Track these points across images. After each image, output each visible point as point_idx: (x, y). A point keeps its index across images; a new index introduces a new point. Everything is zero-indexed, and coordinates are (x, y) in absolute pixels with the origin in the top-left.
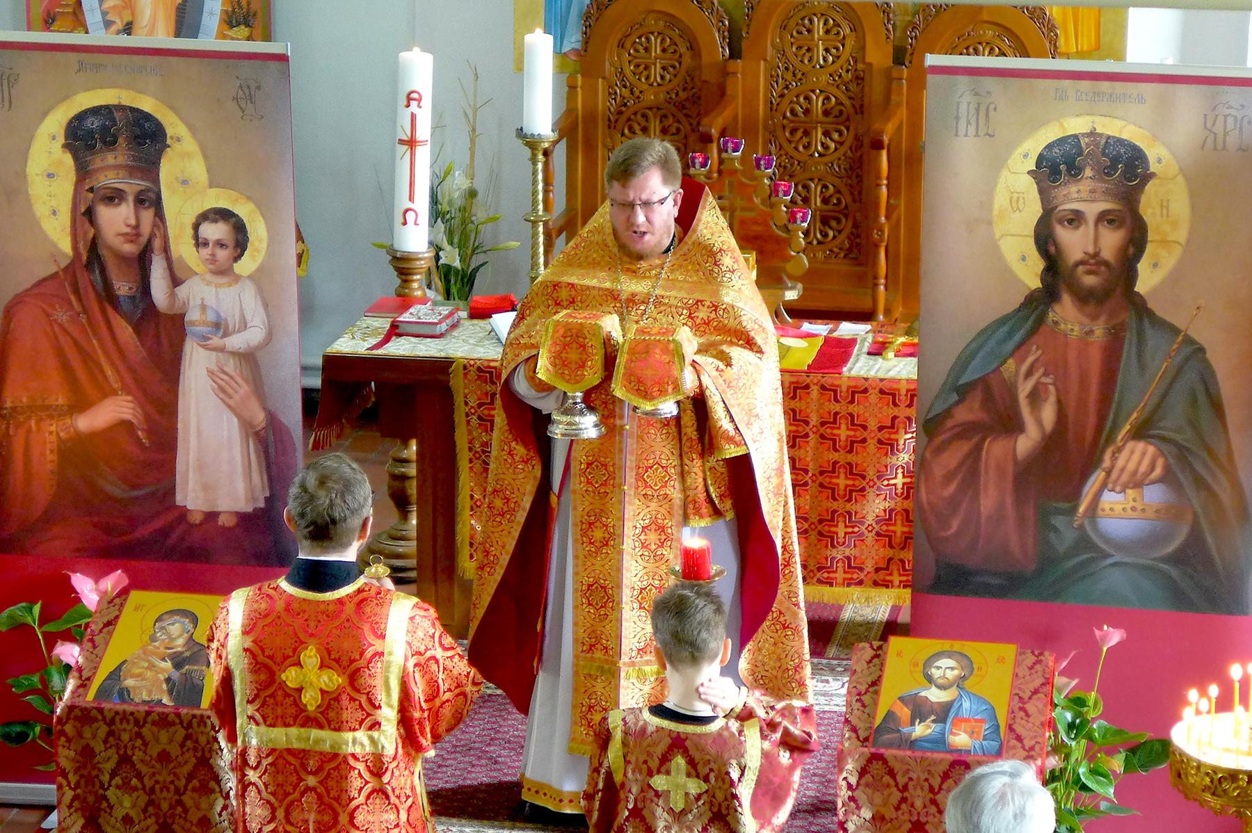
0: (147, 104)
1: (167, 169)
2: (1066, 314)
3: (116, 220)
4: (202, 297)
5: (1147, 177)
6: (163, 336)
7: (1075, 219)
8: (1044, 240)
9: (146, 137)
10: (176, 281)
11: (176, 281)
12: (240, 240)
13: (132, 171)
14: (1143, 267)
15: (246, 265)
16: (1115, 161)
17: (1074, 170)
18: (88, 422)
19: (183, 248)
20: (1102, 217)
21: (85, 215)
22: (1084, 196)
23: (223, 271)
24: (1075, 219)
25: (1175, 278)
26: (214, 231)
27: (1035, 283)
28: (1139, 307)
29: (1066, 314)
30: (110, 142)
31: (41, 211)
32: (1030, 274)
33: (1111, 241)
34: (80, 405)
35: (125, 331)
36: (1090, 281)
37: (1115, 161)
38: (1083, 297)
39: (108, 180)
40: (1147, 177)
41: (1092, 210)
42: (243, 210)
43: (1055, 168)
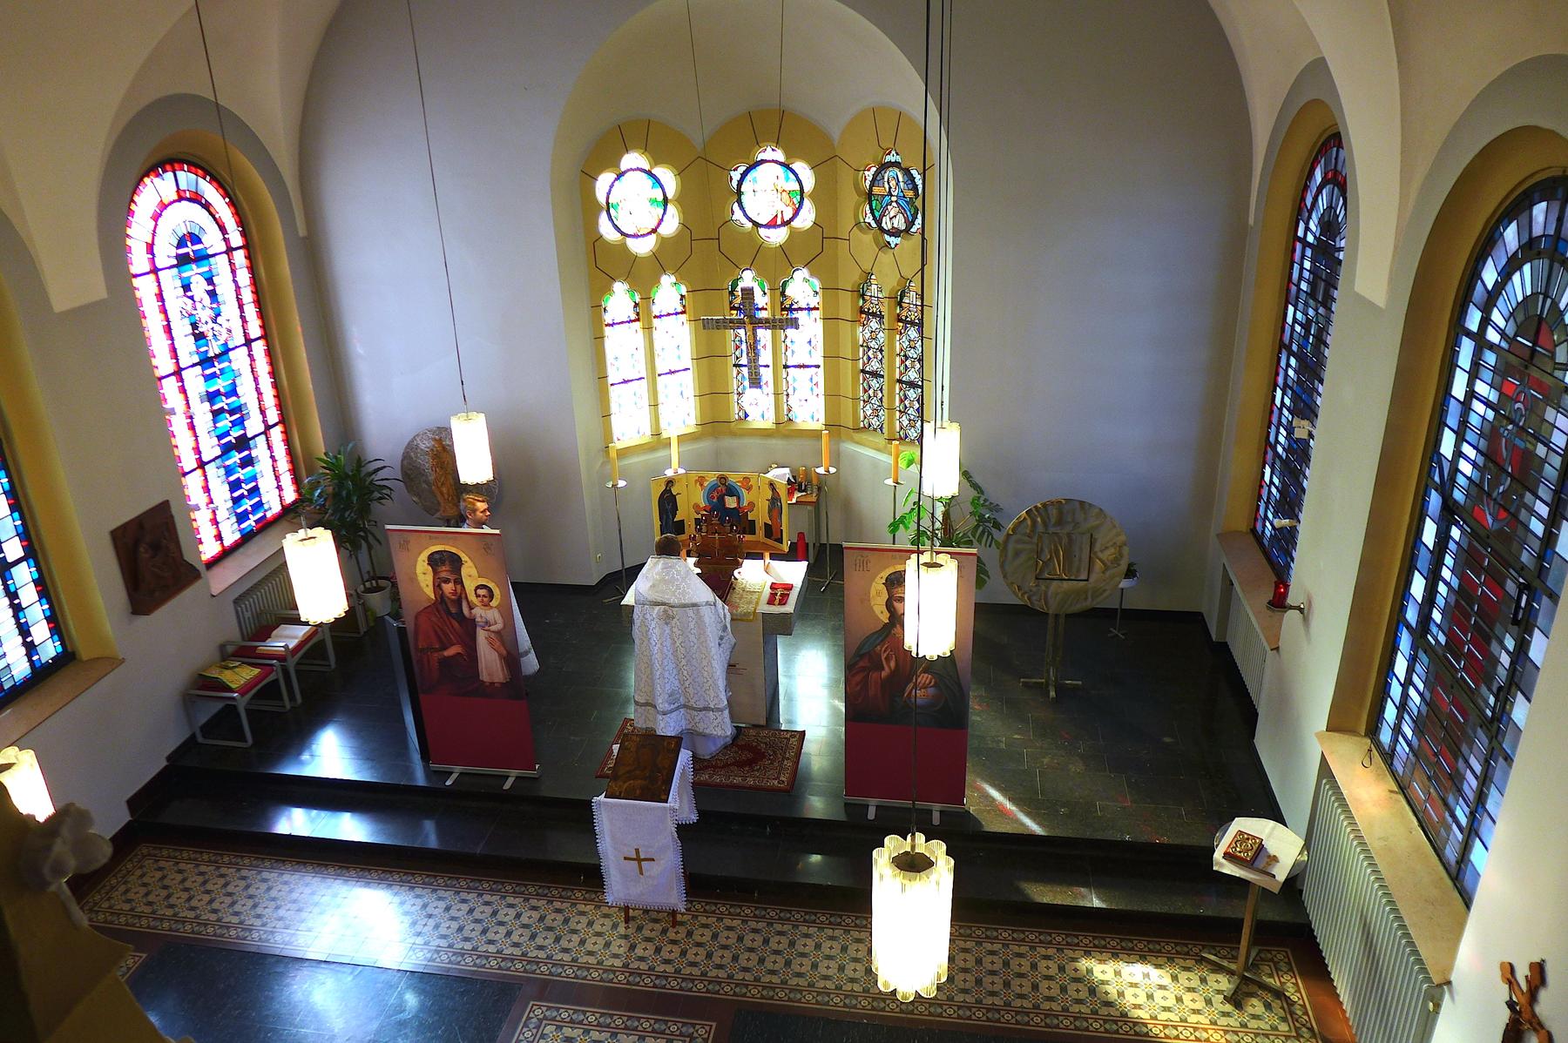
0: (453, 550)
1: (464, 571)
3: (448, 588)
4: (479, 613)
6: (470, 626)
9: (456, 562)
10: (471, 608)
11: (471, 608)
12: (491, 595)
13: (452, 572)
15: (494, 603)
18: (446, 653)
19: (472, 597)
21: (437, 587)
23: (486, 605)
26: (482, 592)
30: (443, 564)
31: (423, 585)
34: (446, 648)
35: (456, 625)
39: (443, 575)
42: (491, 585)
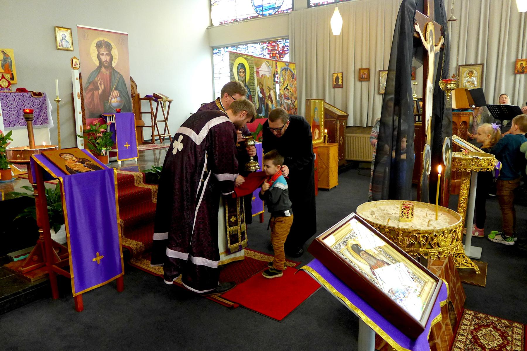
2: (103, 70)
5: (112, 48)
7: (103, 54)
8: (99, 58)
14: (113, 62)
16: (107, 45)
17: (102, 46)
20: (106, 54)
22: (103, 51)
24: (103, 54)
25: (117, 64)
27: (98, 65)
28: (113, 68)
29: (103, 70)
32: (97, 63)
33: (108, 58)
36: (106, 64)
37: (107, 45)
38: (105, 67)
40: (112, 48)
41: (105, 53)
43: (99, 45)
